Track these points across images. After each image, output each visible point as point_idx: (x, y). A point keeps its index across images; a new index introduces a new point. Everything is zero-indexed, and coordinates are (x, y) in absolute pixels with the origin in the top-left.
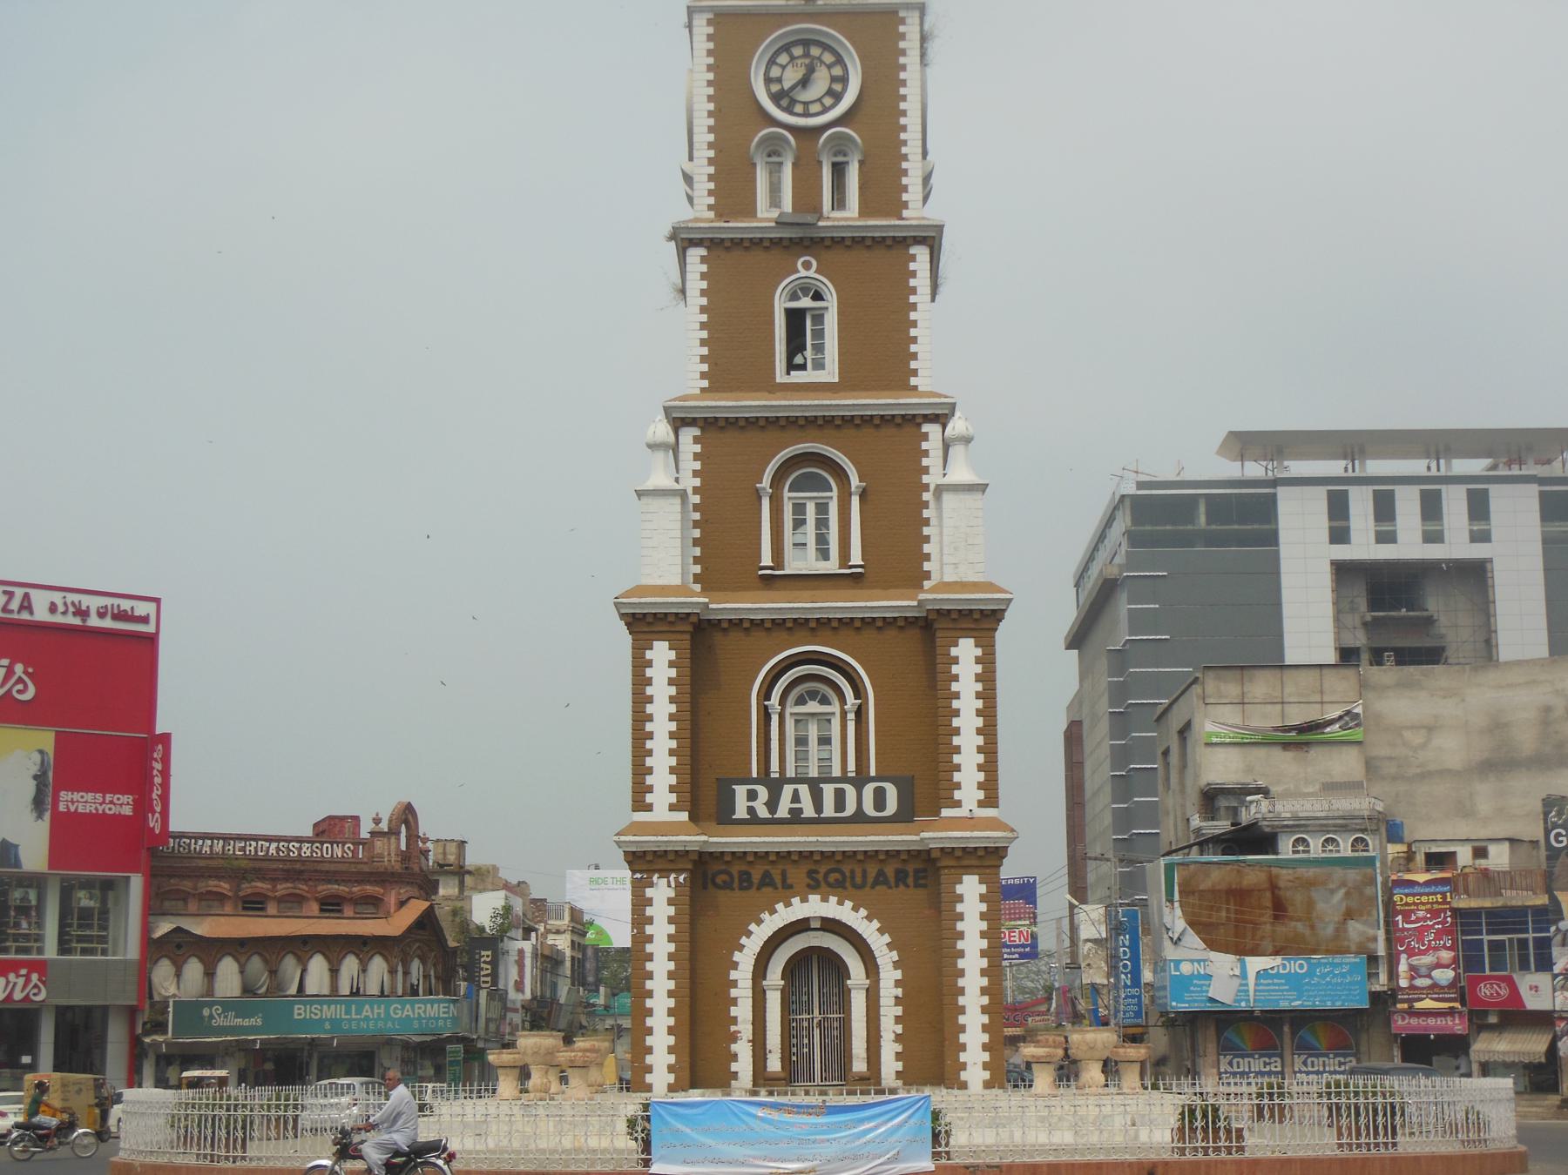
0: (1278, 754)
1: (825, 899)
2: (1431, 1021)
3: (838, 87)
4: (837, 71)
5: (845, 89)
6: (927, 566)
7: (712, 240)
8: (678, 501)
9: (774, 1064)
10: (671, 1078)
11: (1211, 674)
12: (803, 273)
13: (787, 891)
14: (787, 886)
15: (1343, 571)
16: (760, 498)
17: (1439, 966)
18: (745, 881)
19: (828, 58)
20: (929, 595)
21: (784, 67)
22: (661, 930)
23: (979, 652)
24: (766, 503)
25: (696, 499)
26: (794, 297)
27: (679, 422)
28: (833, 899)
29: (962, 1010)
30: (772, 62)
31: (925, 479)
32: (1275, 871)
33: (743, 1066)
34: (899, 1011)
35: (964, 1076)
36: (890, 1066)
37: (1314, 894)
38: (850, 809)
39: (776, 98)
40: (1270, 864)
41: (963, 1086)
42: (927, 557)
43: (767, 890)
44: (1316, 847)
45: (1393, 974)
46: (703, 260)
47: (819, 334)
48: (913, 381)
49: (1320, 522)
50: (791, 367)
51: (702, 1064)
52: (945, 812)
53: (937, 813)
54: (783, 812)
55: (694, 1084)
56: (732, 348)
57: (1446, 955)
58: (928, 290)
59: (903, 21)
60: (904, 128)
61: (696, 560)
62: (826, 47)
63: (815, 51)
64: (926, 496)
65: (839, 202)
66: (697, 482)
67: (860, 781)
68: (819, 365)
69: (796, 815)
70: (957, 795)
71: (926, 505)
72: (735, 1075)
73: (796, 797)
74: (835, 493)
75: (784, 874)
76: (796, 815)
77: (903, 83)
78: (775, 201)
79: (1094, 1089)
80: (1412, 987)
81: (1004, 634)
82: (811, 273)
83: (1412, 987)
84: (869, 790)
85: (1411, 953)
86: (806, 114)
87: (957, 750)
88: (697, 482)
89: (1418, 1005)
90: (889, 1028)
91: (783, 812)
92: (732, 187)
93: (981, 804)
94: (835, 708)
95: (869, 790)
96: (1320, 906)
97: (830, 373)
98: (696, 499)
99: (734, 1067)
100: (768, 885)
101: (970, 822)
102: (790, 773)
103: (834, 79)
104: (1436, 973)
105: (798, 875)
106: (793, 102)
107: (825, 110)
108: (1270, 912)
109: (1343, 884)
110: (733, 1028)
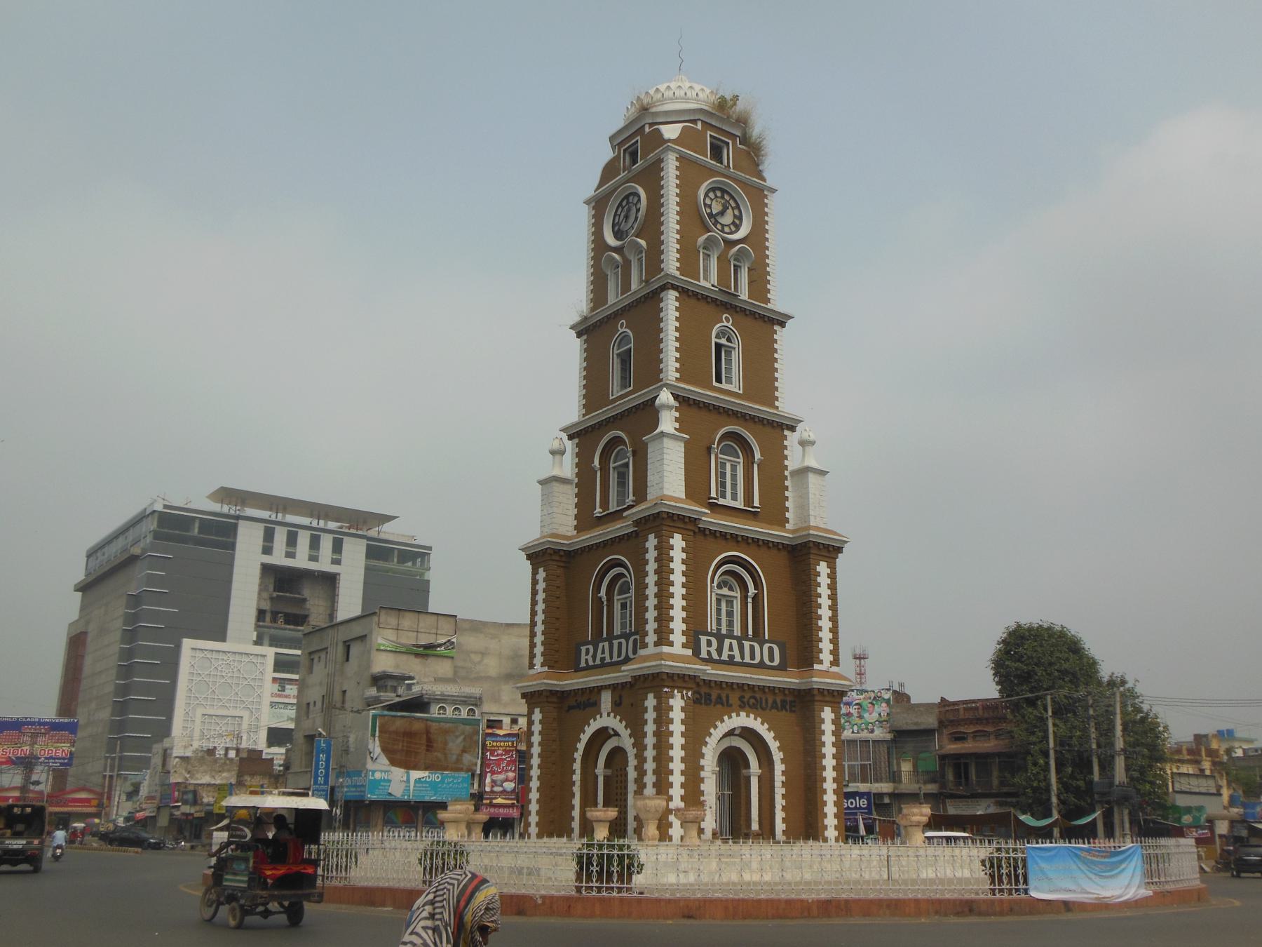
0: (412, 658)
2: (501, 810)
11: (383, 612)
15: (267, 569)
17: (507, 780)
43: (719, 706)
45: (482, 784)
49: (259, 542)
57: (511, 775)
73: (731, 649)
79: (650, 843)
80: (492, 791)
83: (492, 791)
85: (493, 773)
89: (495, 801)
95: (766, 646)
96: (451, 745)
104: (505, 784)
108: (424, 747)
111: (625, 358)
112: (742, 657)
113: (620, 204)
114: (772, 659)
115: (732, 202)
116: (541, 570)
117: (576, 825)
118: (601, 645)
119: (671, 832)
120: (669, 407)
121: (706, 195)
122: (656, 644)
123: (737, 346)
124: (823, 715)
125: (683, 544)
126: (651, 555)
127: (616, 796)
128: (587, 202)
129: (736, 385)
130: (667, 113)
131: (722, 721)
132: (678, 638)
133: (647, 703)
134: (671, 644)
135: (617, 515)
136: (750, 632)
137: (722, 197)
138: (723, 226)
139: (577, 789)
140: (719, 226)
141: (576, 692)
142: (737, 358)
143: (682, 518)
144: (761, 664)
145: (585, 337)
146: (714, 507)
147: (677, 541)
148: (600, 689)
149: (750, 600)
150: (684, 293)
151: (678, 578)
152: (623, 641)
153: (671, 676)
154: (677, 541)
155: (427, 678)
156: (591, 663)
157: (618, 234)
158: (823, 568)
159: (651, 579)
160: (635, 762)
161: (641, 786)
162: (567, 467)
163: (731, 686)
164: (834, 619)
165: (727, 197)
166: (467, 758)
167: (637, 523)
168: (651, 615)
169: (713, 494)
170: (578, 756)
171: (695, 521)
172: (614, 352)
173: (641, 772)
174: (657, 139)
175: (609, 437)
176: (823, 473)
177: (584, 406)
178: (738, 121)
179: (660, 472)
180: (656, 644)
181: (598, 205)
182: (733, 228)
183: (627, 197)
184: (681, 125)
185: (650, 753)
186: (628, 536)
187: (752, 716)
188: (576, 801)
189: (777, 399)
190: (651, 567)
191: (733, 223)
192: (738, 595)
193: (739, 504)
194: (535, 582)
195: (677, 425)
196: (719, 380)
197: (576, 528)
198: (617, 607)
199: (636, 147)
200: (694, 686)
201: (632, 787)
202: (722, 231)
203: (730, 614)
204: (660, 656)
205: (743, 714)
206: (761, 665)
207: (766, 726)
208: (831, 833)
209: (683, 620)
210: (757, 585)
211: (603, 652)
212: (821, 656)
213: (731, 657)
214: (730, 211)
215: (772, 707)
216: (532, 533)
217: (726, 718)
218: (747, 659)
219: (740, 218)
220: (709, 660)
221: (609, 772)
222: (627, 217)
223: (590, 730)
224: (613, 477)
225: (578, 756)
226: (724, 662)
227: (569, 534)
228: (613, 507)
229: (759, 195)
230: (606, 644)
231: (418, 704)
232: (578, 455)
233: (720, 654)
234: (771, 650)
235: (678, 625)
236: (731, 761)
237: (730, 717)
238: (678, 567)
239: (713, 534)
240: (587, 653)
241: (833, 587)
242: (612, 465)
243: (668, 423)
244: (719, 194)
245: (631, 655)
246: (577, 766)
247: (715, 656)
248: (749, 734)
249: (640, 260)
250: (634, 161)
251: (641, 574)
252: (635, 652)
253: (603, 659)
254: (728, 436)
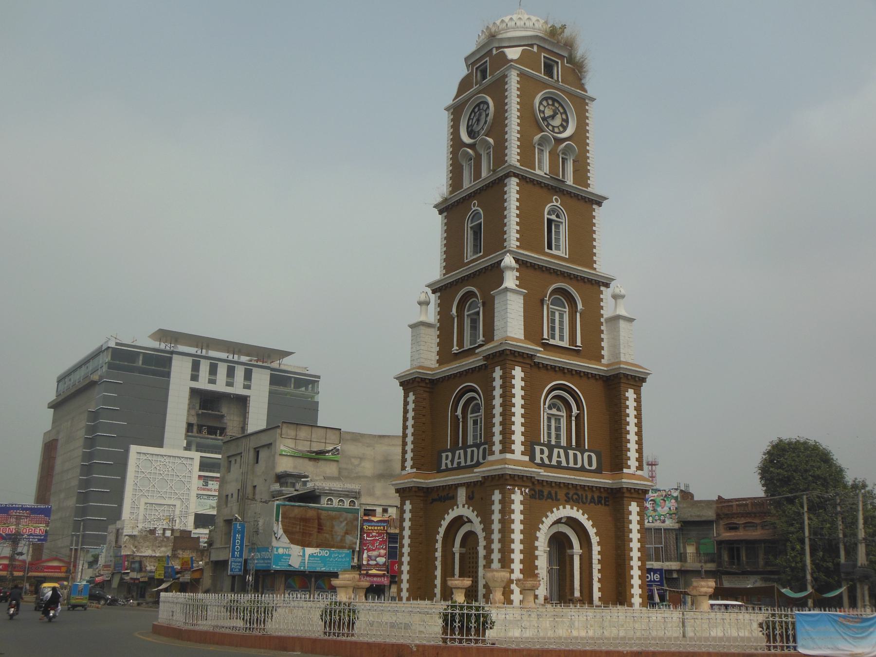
0: (307, 461)
2: (375, 579)
11: (285, 425)
12: (555, 204)
15: (194, 392)
17: (379, 556)
37: (335, 523)
40: (318, 509)
43: (549, 500)
44: (335, 502)
45: (360, 558)
57: (383, 552)
73: (559, 456)
75: (556, 493)
80: (368, 564)
83: (368, 564)
85: (369, 550)
89: (370, 572)
95: (586, 454)
96: (337, 528)
104: (378, 559)
108: (316, 530)
109: (346, 519)
111: (477, 230)
112: (568, 462)
113: (473, 111)
114: (590, 464)
115: (560, 108)
116: (411, 394)
117: (438, 591)
118: (457, 452)
119: (512, 597)
120: (512, 269)
121: (541, 103)
122: (501, 452)
123: (564, 221)
124: (631, 508)
125: (522, 375)
126: (498, 383)
127: (469, 568)
128: (447, 109)
129: (563, 251)
130: (510, 39)
131: (552, 512)
132: (518, 448)
133: (493, 498)
134: (513, 452)
135: (471, 352)
136: (574, 443)
137: (553, 105)
138: (553, 127)
139: (438, 564)
140: (550, 128)
141: (438, 488)
142: (564, 230)
143: (521, 355)
144: (582, 467)
145: (445, 214)
146: (546, 346)
147: (518, 373)
148: (457, 486)
149: (573, 418)
150: (524, 180)
151: (518, 401)
152: (475, 449)
153: (512, 477)
154: (518, 373)
156: (450, 466)
157: (471, 133)
158: (630, 394)
159: (497, 402)
160: (484, 543)
161: (489, 561)
162: (431, 315)
163: (559, 485)
164: (639, 434)
165: (556, 105)
166: (349, 539)
167: (486, 358)
168: (497, 429)
169: (545, 336)
170: (440, 538)
171: (531, 357)
172: (468, 225)
173: (489, 550)
174: (503, 60)
175: (464, 291)
176: (631, 320)
177: (445, 267)
178: (566, 45)
179: (505, 318)
180: (501, 452)
181: (456, 111)
182: (561, 129)
183: (478, 105)
184: (521, 49)
185: (496, 536)
186: (480, 367)
187: (575, 508)
188: (438, 573)
189: (595, 262)
190: (498, 392)
191: (561, 125)
192: (565, 415)
193: (565, 344)
194: (406, 403)
195: (518, 282)
196: (550, 247)
197: (438, 361)
198: (470, 423)
199: (486, 67)
200: (530, 485)
201: (482, 562)
202: (553, 131)
203: (558, 429)
204: (504, 461)
205: (568, 507)
206: (582, 469)
207: (586, 516)
208: (637, 600)
209: (522, 434)
210: (579, 406)
211: (459, 458)
212: (629, 463)
213: (559, 462)
214: (559, 116)
215: (591, 502)
216: (404, 366)
217: (555, 509)
218: (571, 464)
219: (567, 121)
220: (542, 465)
221: (464, 550)
222: (478, 120)
223: (449, 518)
224: (467, 323)
225: (440, 538)
227: (433, 366)
228: (467, 346)
229: (582, 103)
230: (462, 452)
231: (312, 497)
232: (439, 305)
233: (550, 460)
234: (590, 457)
235: (518, 438)
236: (559, 543)
237: (558, 509)
238: (518, 392)
239: (545, 367)
240: (447, 459)
241: (638, 409)
242: (466, 313)
243: (510, 280)
244: (550, 102)
245: (481, 460)
246: (439, 546)
247: (547, 461)
248: (572, 522)
249: (489, 154)
250: (484, 77)
251: (489, 398)
252: (484, 458)
253: (459, 463)
254: (557, 291)
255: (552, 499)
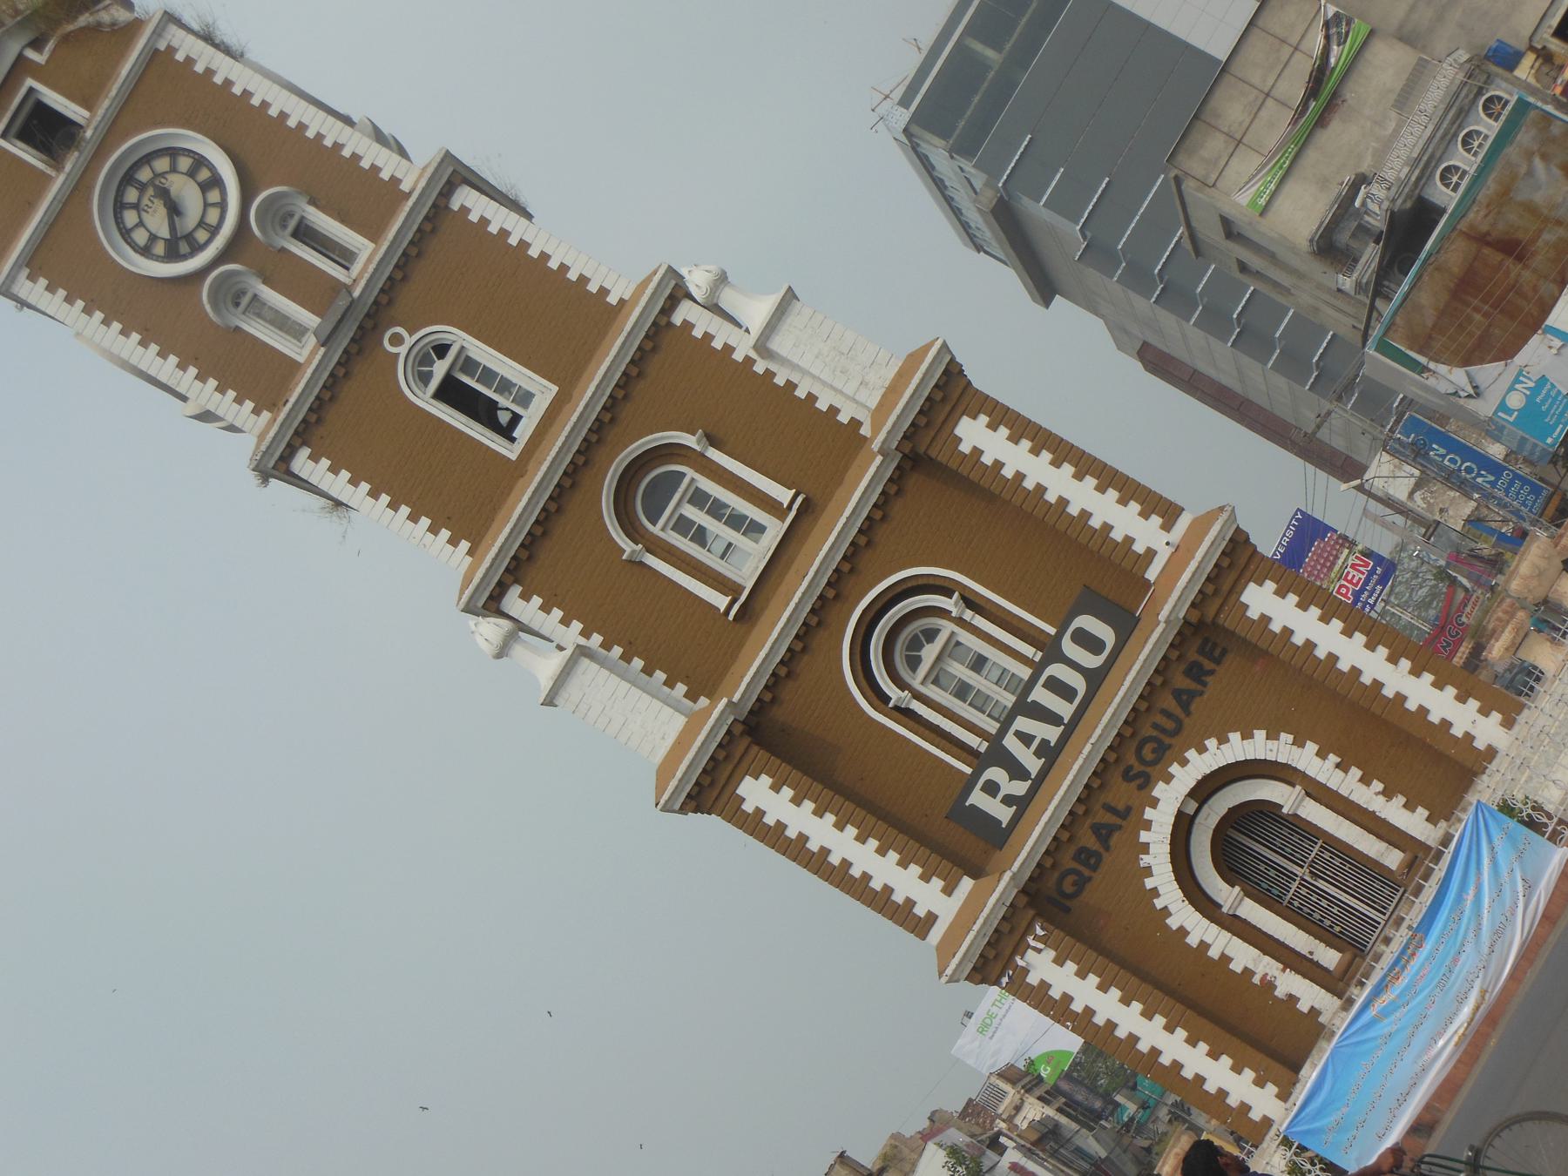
0: (1324, 137)
1: (1168, 778)
3: (204, 174)
4: (184, 163)
5: (212, 168)
6: (843, 418)
7: (296, 433)
8: (585, 662)
9: (1330, 958)
10: (1271, 1089)
11: (1181, 157)
12: (402, 350)
13: (1130, 818)
14: (1125, 813)
16: (641, 563)
18: (1090, 859)
19: (162, 164)
20: (879, 436)
21: (141, 224)
22: (1086, 992)
23: (983, 419)
24: (652, 561)
25: (597, 639)
26: (425, 378)
27: (492, 605)
28: (1175, 769)
29: (1401, 698)
30: (126, 234)
31: (738, 356)
32: (1462, 226)
33: (1309, 995)
34: (1356, 773)
35: (1480, 744)
36: (1414, 823)
38: (1078, 683)
39: (172, 255)
40: (1452, 227)
41: (1491, 752)
42: (834, 411)
43: (1115, 839)
46: (315, 458)
47: (488, 376)
48: (612, 299)
50: (507, 432)
51: (1279, 1044)
52: (1152, 574)
53: (1147, 584)
54: (1033, 765)
55: (1295, 1067)
56: (440, 489)
58: (514, 216)
59: (171, 50)
60: (302, 127)
61: (670, 683)
62: (147, 159)
63: (144, 175)
64: (760, 367)
65: (344, 257)
66: (577, 626)
67: (1052, 652)
68: (525, 398)
69: (1044, 750)
70: (1139, 548)
71: (769, 374)
72: (1315, 1012)
73: (1026, 739)
74: (690, 473)
76: (1044, 750)
77: (247, 94)
78: (297, 331)
81: (980, 377)
82: (409, 340)
84: (1069, 648)
86: (214, 231)
87: (1085, 515)
88: (577, 626)
90: (1368, 796)
91: (1033, 765)
92: (248, 372)
93: (1167, 527)
94: (947, 628)
95: (1069, 648)
96: (1539, 198)
97: (544, 392)
98: (597, 639)
99: (1303, 1007)
100: (1110, 834)
101: (1181, 553)
102: (992, 727)
103: (191, 174)
105: (1120, 793)
106: (189, 237)
107: (223, 206)
108: (1509, 262)
109: (1529, 155)
110: (1256, 980)
155: (1386, 139)
226: (1044, 773)
255: (1120, 827)
